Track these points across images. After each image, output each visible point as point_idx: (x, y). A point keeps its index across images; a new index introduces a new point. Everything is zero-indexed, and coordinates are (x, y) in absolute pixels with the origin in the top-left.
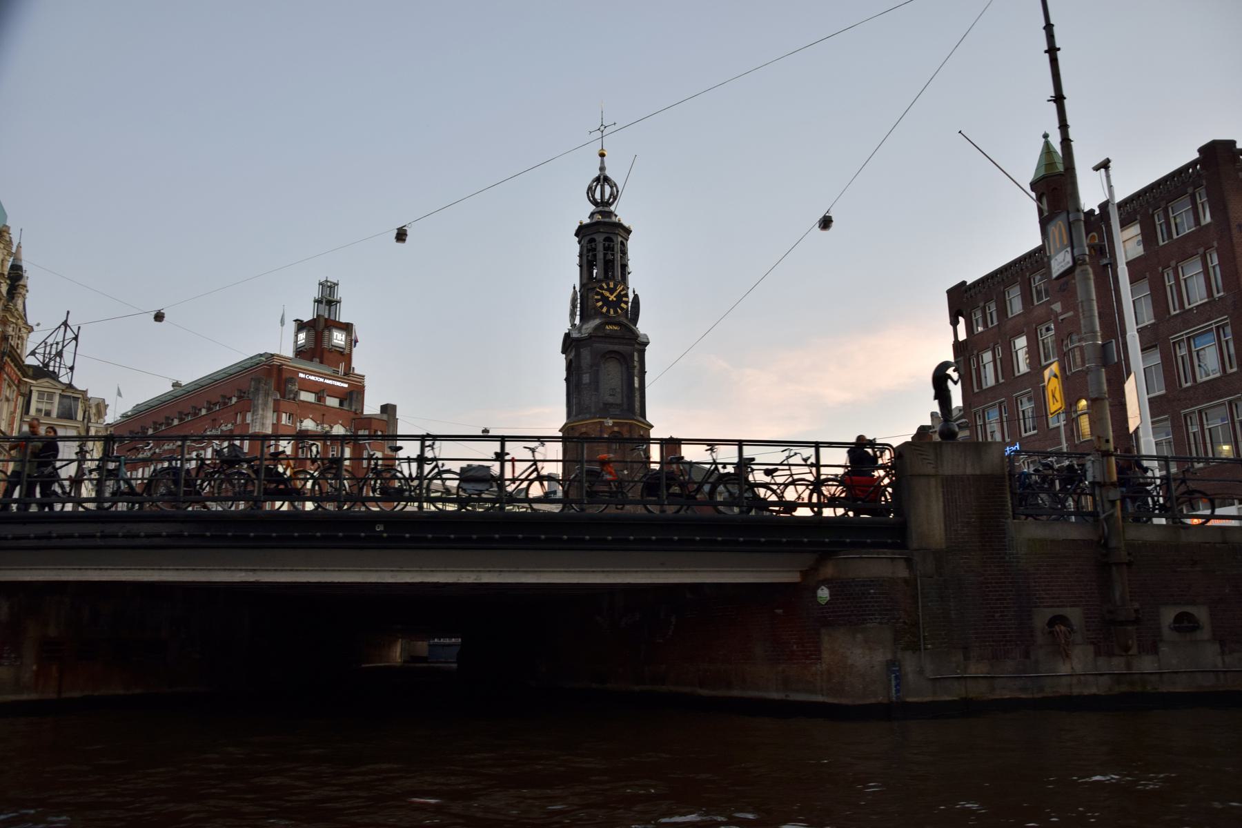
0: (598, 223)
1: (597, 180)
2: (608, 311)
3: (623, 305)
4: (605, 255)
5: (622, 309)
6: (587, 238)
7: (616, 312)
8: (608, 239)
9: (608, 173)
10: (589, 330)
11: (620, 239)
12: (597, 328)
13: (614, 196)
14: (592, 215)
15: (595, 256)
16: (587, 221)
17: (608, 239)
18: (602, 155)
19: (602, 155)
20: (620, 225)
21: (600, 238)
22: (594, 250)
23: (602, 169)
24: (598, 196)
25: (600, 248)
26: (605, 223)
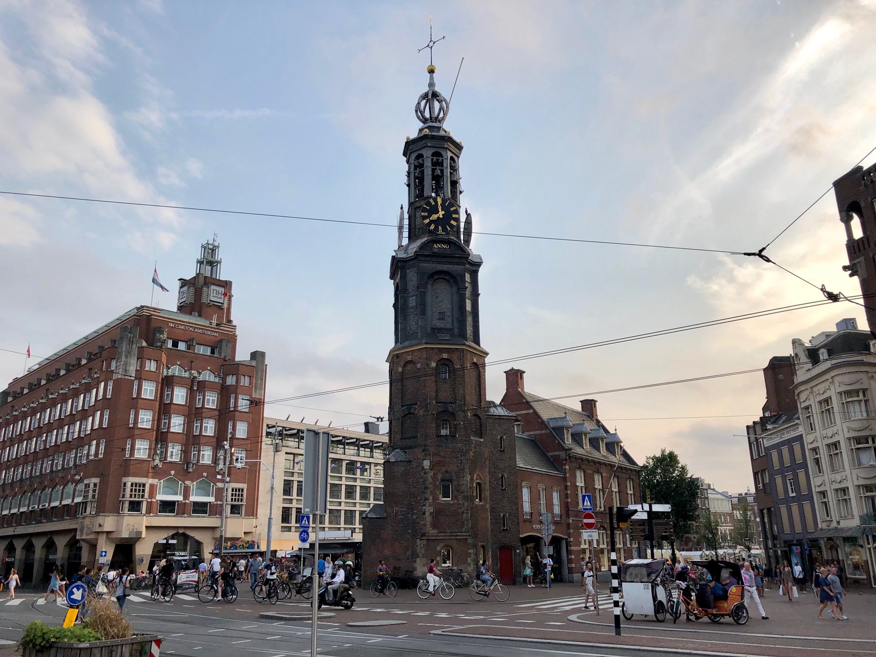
0: (425, 137)
1: (425, 96)
2: (436, 229)
3: (453, 222)
4: (433, 170)
5: (452, 226)
6: (413, 156)
7: (444, 229)
8: (437, 154)
9: (437, 89)
10: (415, 250)
11: (450, 154)
12: (422, 247)
13: (444, 110)
14: (421, 130)
15: (422, 172)
16: (414, 135)
17: (437, 154)
18: (431, 71)
19: (431, 71)
20: (450, 140)
21: (427, 153)
22: (421, 166)
23: (431, 85)
24: (427, 115)
25: (428, 164)
26: (433, 137)
